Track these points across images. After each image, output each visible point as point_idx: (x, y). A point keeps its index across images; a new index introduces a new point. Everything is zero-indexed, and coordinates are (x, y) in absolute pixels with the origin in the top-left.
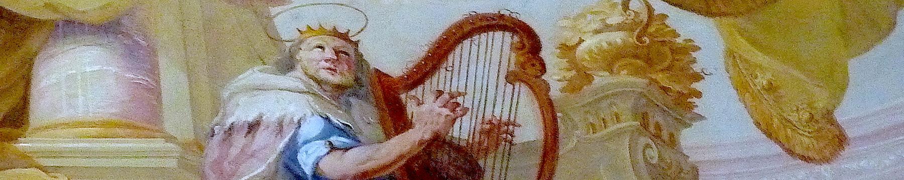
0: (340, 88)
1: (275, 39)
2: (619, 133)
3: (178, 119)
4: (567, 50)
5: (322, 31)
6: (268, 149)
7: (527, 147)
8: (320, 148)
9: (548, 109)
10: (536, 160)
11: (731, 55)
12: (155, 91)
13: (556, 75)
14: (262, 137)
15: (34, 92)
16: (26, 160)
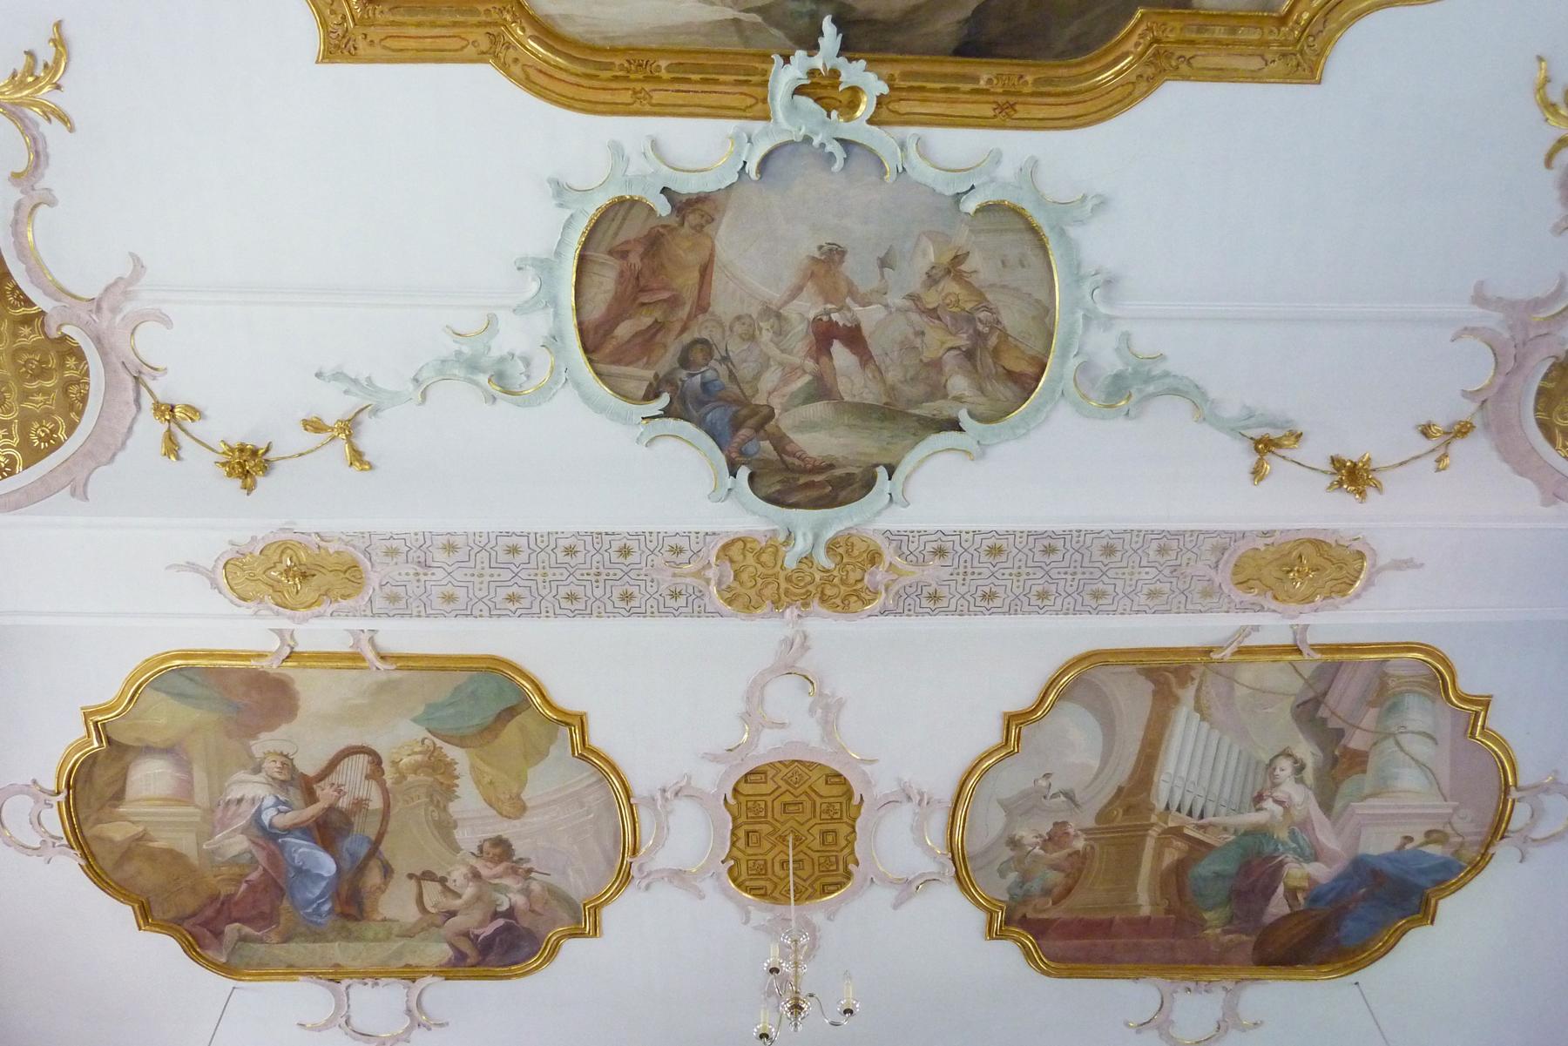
0: (283, 781)
1: (251, 757)
2: (418, 805)
3: (201, 795)
4: (395, 763)
5: (275, 753)
6: (248, 811)
7: (375, 812)
8: (273, 812)
9: (385, 792)
10: (378, 819)
11: (473, 767)
12: (190, 782)
13: (389, 776)
14: (244, 806)
15: (129, 782)
16: (123, 818)
